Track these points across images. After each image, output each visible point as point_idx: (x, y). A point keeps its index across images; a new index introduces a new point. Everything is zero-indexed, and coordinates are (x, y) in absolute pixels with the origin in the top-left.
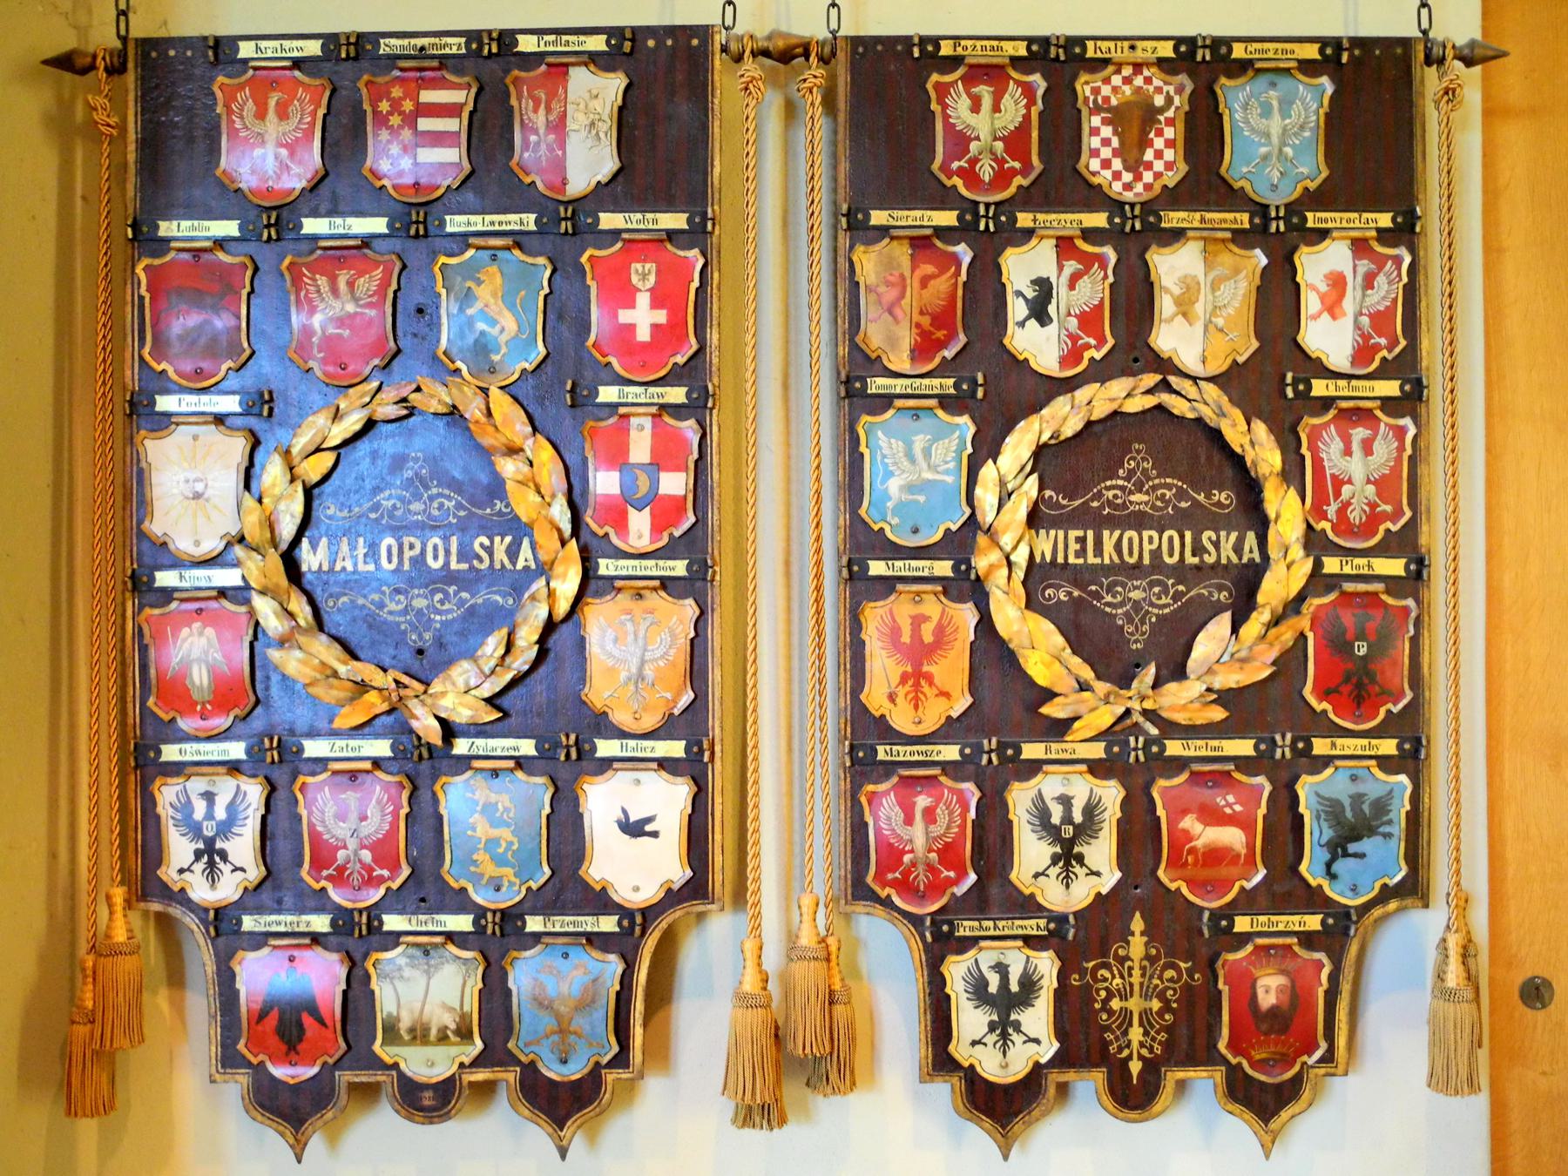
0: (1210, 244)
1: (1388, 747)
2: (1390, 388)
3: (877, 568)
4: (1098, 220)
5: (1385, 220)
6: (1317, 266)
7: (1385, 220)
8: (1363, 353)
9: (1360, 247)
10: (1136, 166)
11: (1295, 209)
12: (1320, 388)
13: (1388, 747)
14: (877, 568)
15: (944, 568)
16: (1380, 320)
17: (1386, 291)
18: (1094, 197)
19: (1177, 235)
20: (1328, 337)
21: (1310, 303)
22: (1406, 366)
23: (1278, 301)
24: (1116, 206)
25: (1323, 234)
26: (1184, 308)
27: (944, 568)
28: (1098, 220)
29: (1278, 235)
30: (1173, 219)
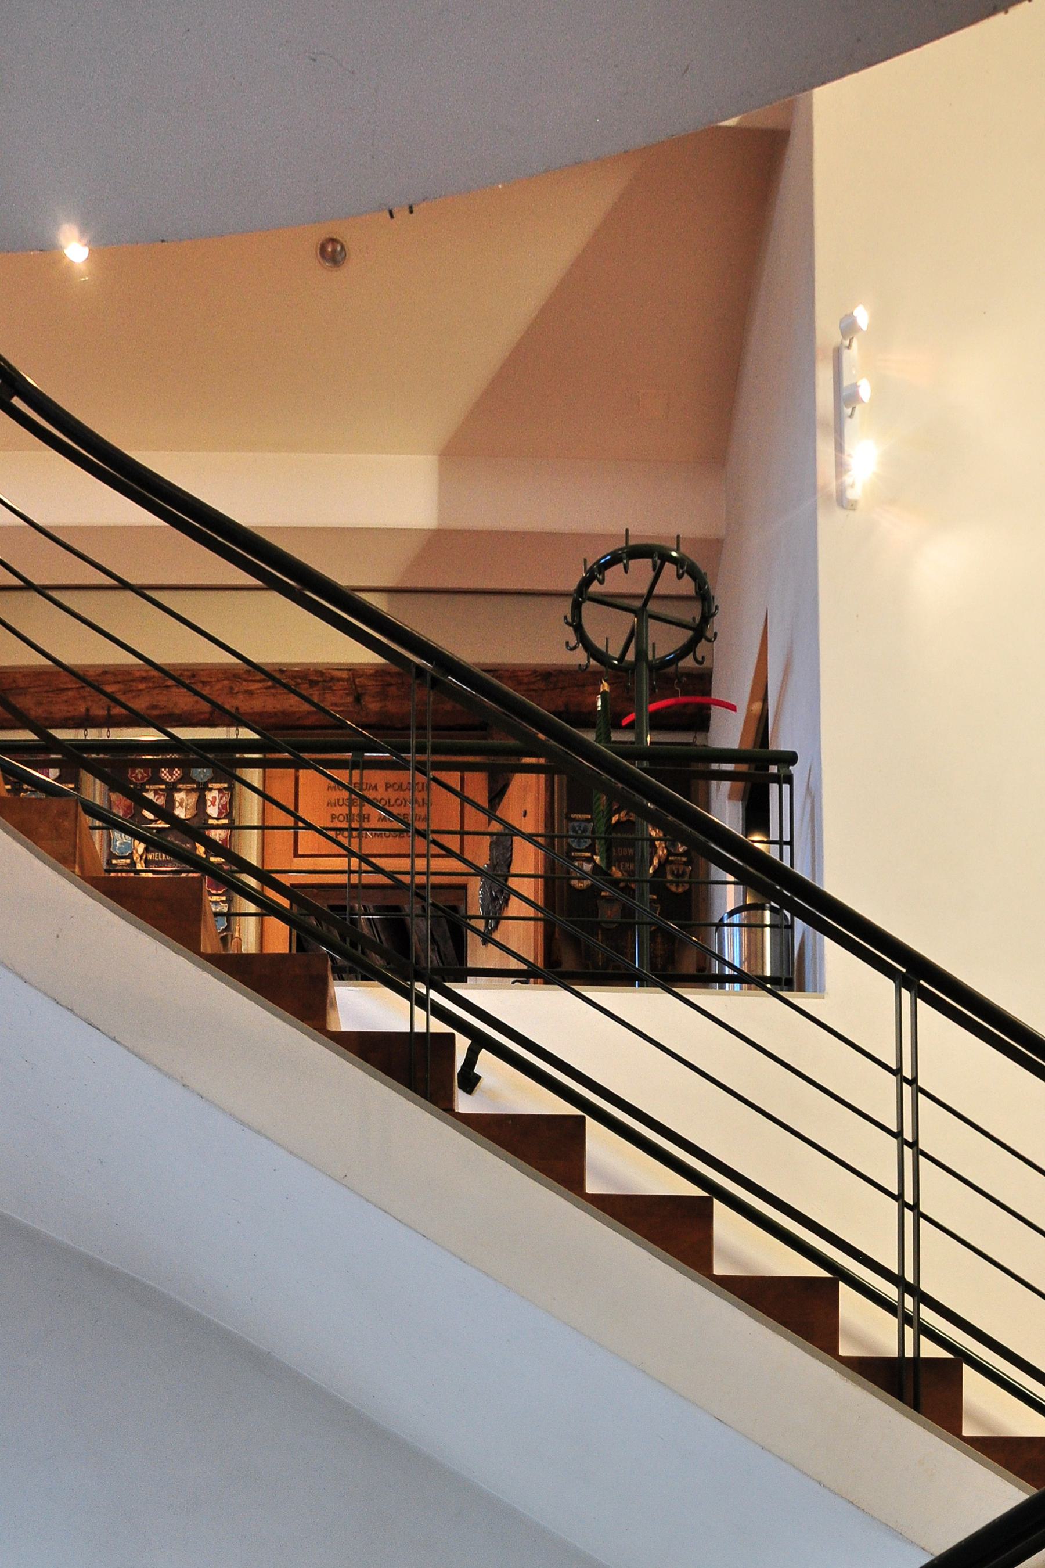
0: (188, 791)
1: (224, 898)
2: (226, 821)
3: (114, 862)
4: (163, 787)
5: (226, 785)
6: (210, 796)
7: (226, 785)
8: (220, 813)
9: (220, 790)
10: (171, 775)
11: (206, 783)
12: (211, 822)
13: (224, 898)
14: (114, 862)
15: (128, 861)
16: (224, 807)
17: (225, 800)
18: (163, 782)
19: (180, 790)
20: (213, 811)
21: (209, 803)
22: (229, 815)
23: (201, 803)
24: (166, 783)
25: (211, 789)
26: (181, 805)
27: (128, 861)
28: (163, 787)
29: (202, 789)
30: (180, 786)
